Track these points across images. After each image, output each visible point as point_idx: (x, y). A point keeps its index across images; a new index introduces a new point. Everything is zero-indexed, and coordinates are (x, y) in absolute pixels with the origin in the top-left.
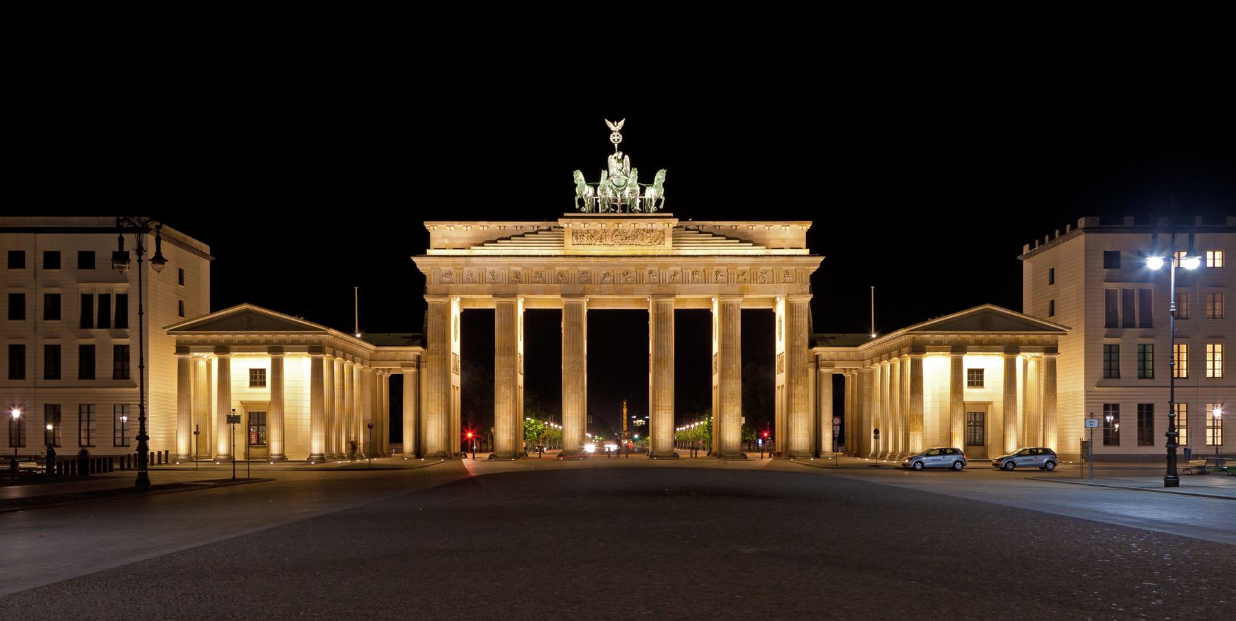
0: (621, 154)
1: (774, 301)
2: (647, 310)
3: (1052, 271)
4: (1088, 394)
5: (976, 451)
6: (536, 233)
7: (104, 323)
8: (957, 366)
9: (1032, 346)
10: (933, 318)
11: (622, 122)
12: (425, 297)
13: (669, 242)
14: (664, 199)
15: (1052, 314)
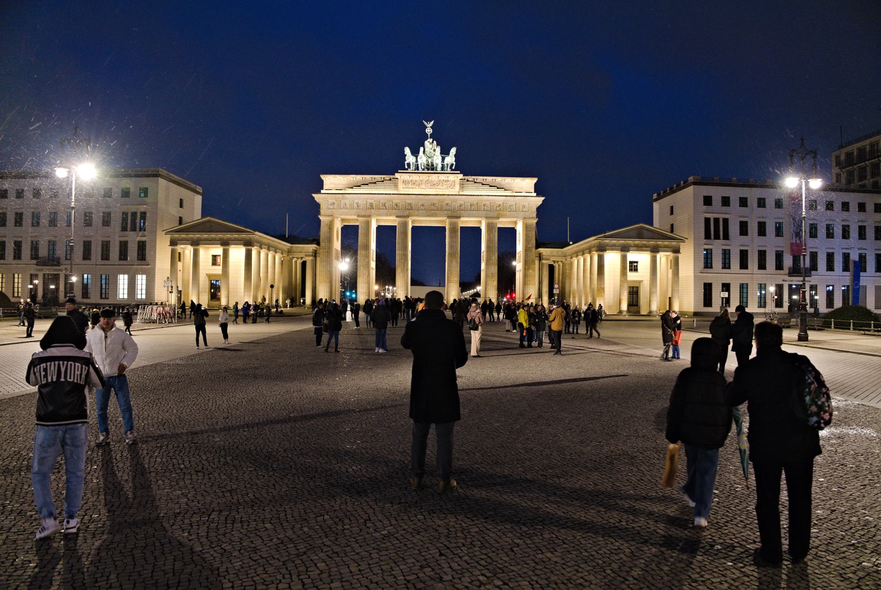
0: (432, 140)
1: (516, 223)
2: (445, 227)
3: (672, 208)
4: (695, 276)
5: (634, 309)
6: (383, 181)
7: (134, 229)
8: (624, 258)
9: (666, 248)
10: (610, 231)
11: (433, 122)
12: (319, 216)
13: (457, 187)
14: (454, 163)
15: (672, 231)
